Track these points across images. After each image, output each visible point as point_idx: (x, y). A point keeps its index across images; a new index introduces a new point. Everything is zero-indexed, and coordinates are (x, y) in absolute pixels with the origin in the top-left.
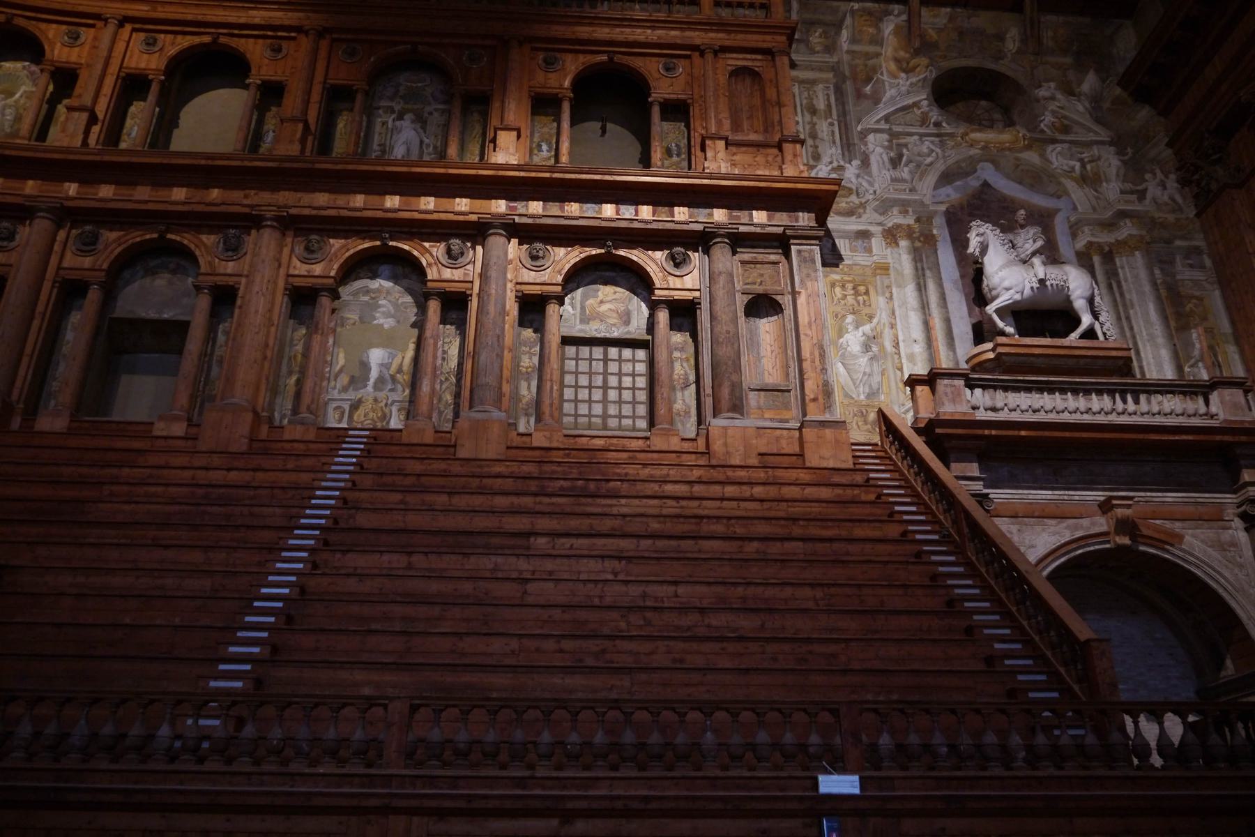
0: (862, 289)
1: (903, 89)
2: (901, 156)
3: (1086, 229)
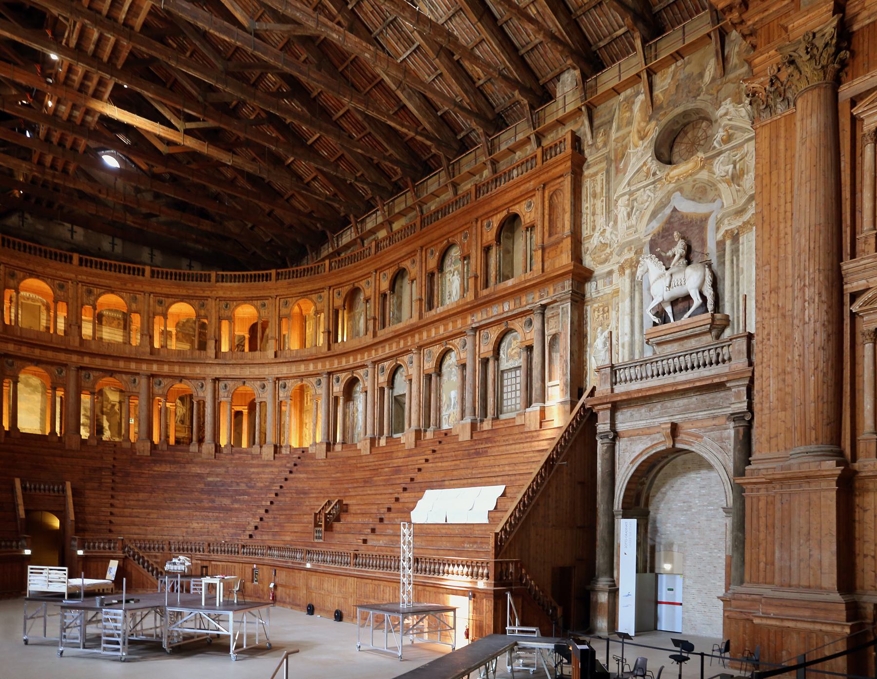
0: (606, 309)
1: (640, 154)
2: (632, 209)
3: (726, 222)
